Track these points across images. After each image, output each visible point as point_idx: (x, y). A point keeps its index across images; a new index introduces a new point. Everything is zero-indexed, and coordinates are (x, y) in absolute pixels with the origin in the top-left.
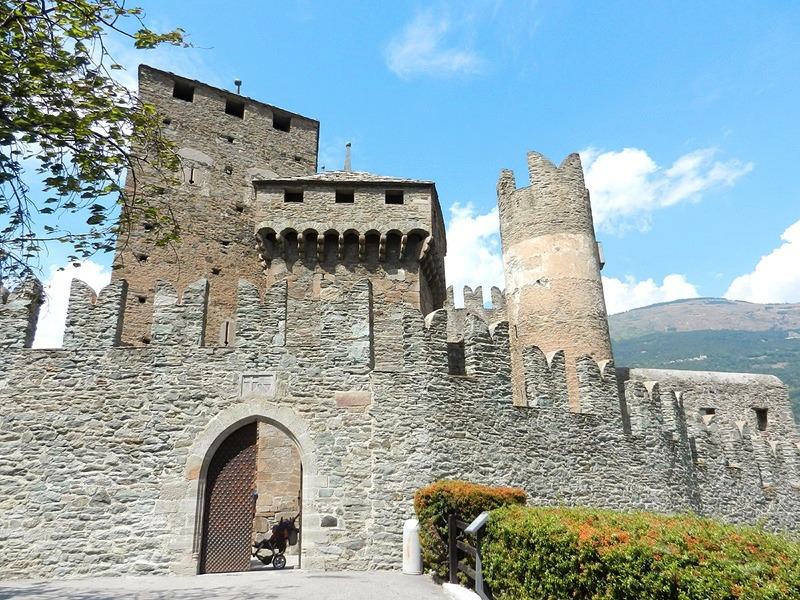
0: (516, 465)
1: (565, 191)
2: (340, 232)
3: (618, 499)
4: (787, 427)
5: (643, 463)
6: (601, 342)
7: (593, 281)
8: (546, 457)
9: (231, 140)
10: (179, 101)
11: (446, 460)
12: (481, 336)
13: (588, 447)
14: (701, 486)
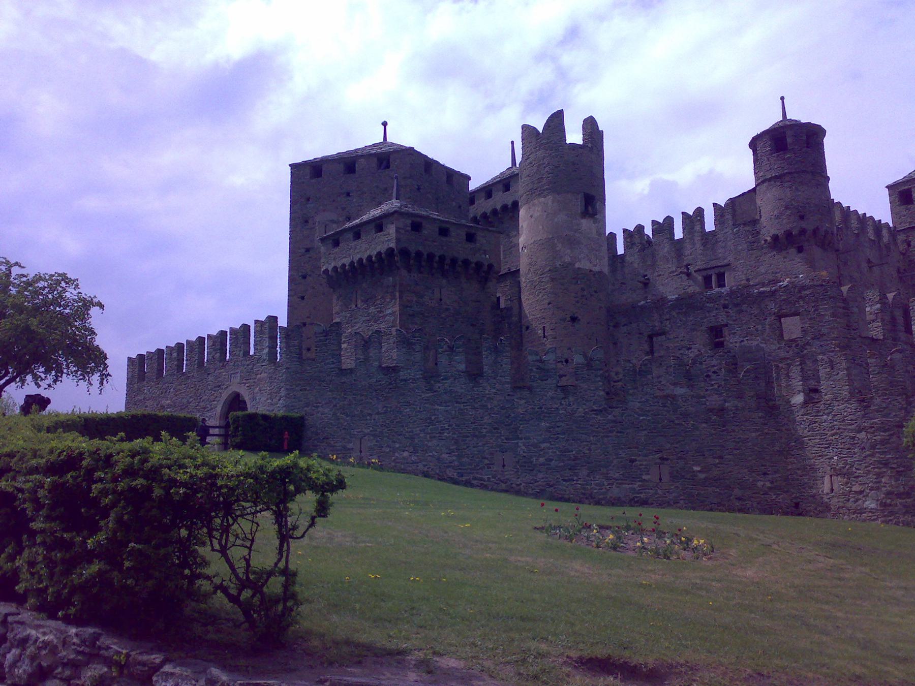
5: (435, 392)
9: (348, 194)
10: (314, 181)
11: (293, 402)
13: (391, 386)
14: (523, 401)
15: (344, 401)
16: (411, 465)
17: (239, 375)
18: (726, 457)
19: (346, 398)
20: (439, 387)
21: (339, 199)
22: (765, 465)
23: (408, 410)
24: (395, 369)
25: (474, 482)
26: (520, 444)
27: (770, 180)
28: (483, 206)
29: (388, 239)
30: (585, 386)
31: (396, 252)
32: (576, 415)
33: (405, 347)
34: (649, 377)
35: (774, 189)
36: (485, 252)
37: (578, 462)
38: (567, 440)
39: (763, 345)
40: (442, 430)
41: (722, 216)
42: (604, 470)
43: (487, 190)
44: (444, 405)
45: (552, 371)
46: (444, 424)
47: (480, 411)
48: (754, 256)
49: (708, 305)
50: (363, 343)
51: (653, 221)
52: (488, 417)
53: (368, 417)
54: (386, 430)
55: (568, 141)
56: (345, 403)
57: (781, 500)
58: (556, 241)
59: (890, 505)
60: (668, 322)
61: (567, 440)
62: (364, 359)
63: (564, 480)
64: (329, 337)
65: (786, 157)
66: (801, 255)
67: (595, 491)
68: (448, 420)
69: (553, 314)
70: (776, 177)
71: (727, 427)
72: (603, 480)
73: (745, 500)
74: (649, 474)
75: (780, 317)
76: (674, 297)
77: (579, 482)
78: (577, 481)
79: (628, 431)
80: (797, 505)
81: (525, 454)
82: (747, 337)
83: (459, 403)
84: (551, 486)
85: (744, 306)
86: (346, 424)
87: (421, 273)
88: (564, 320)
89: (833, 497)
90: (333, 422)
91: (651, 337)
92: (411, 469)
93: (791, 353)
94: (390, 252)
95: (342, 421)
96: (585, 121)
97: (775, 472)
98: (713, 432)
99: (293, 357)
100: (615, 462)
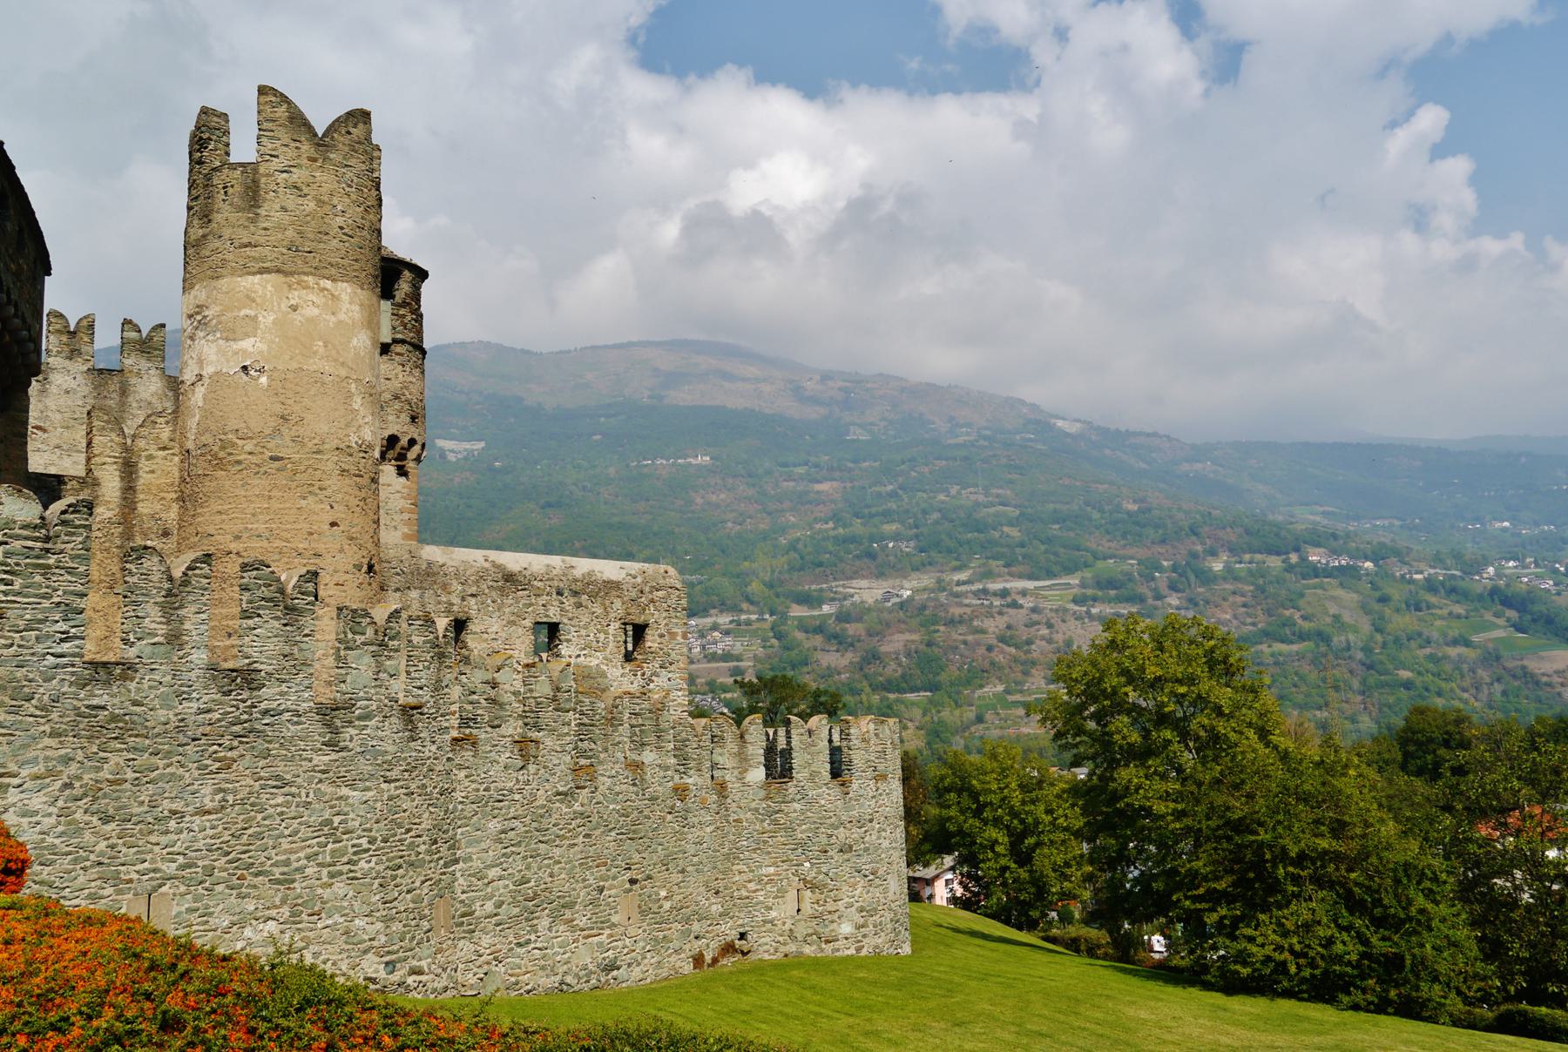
0: (74, 767)
1: (326, 188)
3: (282, 813)
4: (673, 654)
7: (357, 380)
8: (144, 750)
12: (23, 527)
14: (462, 774)
15: (98, 769)
30: (549, 742)
32: (536, 804)
33: (277, 618)
38: (525, 858)
40: (355, 853)
42: (568, 914)
44: (361, 785)
45: (507, 707)
46: (359, 837)
49: (535, 583)
50: (167, 586)
53: (172, 824)
54: (225, 859)
60: (473, 601)
61: (525, 858)
62: (166, 636)
63: (519, 945)
64: (60, 546)
65: (401, 313)
66: (403, 480)
68: (368, 826)
69: (341, 551)
72: (567, 934)
77: (538, 945)
78: (536, 941)
79: (597, 832)
80: (742, 936)
82: (584, 649)
89: (799, 920)
90: (57, 841)
93: (635, 685)
95: (88, 837)
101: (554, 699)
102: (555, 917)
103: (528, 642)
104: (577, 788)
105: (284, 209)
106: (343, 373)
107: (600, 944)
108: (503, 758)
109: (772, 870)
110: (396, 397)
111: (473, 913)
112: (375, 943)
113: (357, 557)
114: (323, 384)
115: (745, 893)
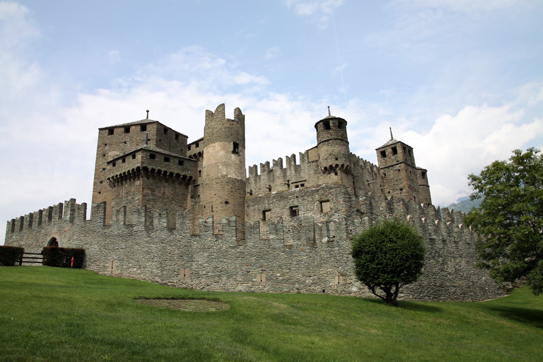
1: (213, 125)
2: (122, 173)
4: (340, 208)
5: (151, 237)
6: (220, 189)
9: (125, 143)
10: (109, 136)
13: (129, 234)
14: (196, 242)
16: (137, 275)
17: (56, 228)
18: (292, 269)
19: (106, 240)
20: (153, 235)
21: (121, 145)
22: (310, 272)
23: (137, 247)
24: (131, 226)
25: (169, 284)
26: (193, 264)
27: (323, 142)
28: (194, 150)
29: (137, 162)
30: (226, 234)
31: (141, 168)
33: (137, 215)
34: (258, 230)
35: (325, 146)
36: (188, 170)
37: (222, 273)
39: (314, 216)
41: (303, 158)
42: (234, 277)
43: (197, 143)
44: (155, 244)
47: (173, 247)
48: (317, 176)
51: (273, 160)
52: (178, 250)
53: (117, 250)
55: (226, 118)
56: (106, 243)
57: (317, 289)
58: (219, 164)
59: (363, 289)
60: (272, 205)
63: (215, 282)
66: (336, 176)
67: (230, 287)
69: (217, 200)
70: (325, 141)
71: (293, 254)
73: (300, 290)
74: (256, 278)
75: (321, 202)
76: (275, 192)
77: (222, 283)
78: (221, 282)
79: (247, 257)
80: (324, 291)
81: (196, 269)
82: (306, 211)
83: (164, 243)
84: (208, 286)
85: (305, 197)
86: (105, 254)
87: (154, 179)
88: (222, 203)
91: (264, 212)
92: (137, 277)
93: (325, 219)
94: (138, 167)
95: (103, 252)
96: (235, 109)
97: (314, 275)
98: (286, 256)
99: (81, 219)
100: (240, 272)
101: (228, 224)
102: (228, 278)
103: (288, 212)
104: (239, 245)
105: (207, 133)
106: (216, 162)
107: (248, 286)
108: (209, 239)
109: (331, 270)
110: (330, 155)
111: (199, 273)
112: (158, 275)
113: (220, 201)
114: (213, 165)
115: (324, 278)
